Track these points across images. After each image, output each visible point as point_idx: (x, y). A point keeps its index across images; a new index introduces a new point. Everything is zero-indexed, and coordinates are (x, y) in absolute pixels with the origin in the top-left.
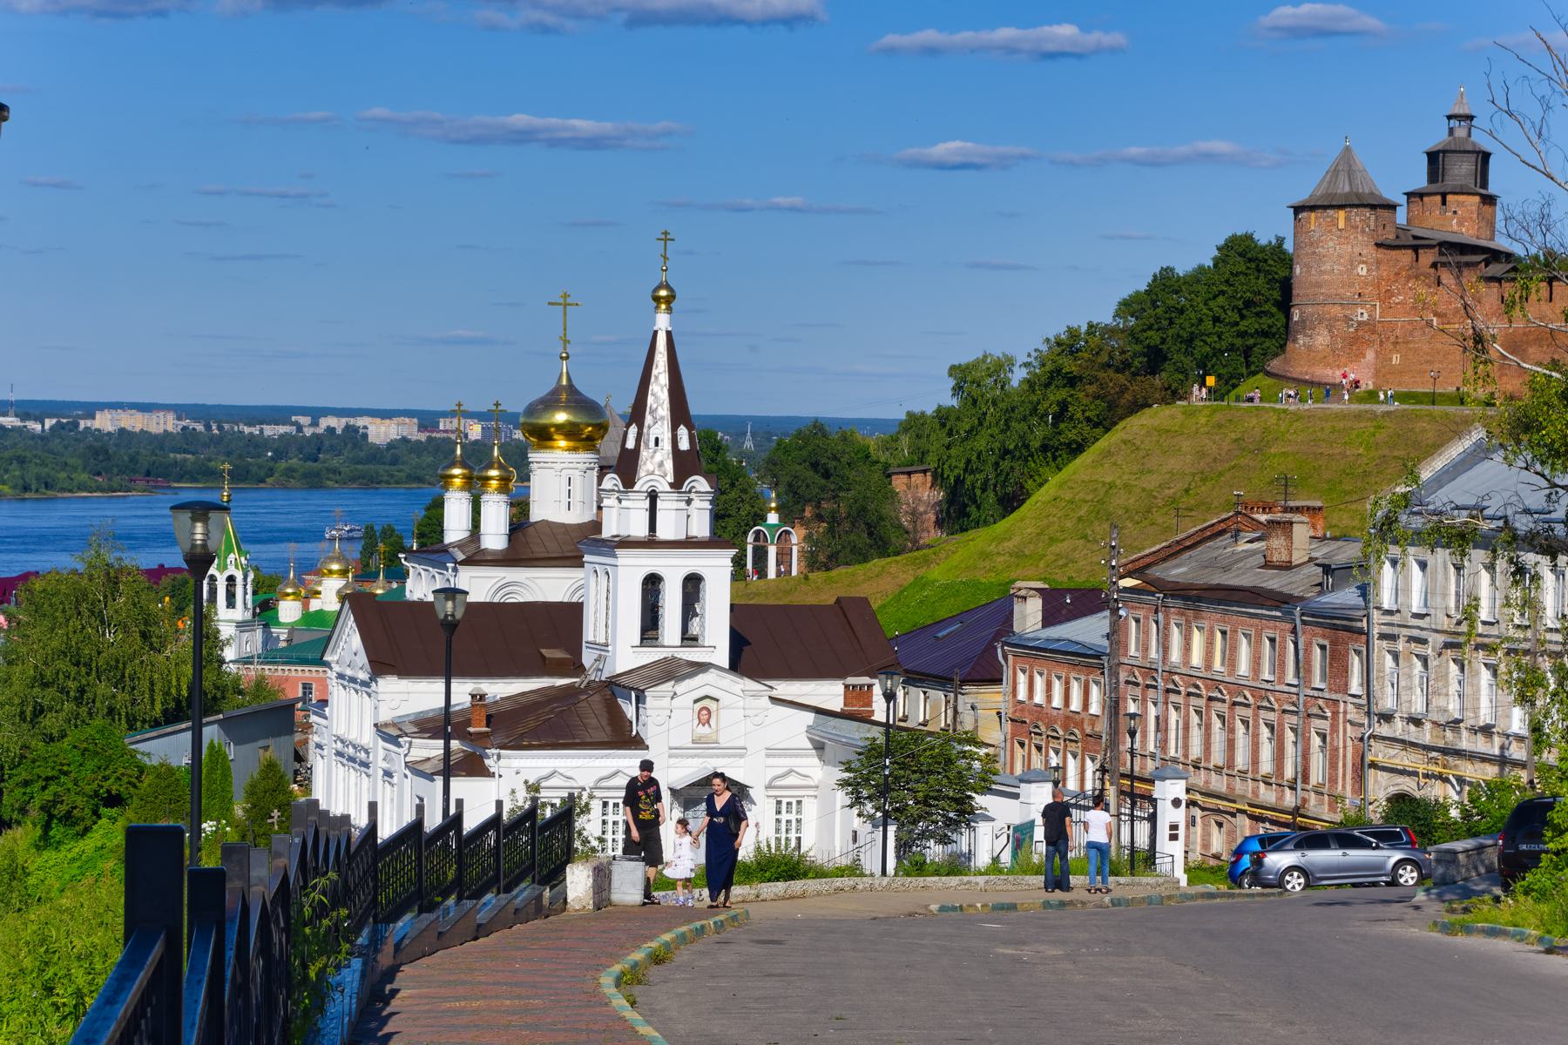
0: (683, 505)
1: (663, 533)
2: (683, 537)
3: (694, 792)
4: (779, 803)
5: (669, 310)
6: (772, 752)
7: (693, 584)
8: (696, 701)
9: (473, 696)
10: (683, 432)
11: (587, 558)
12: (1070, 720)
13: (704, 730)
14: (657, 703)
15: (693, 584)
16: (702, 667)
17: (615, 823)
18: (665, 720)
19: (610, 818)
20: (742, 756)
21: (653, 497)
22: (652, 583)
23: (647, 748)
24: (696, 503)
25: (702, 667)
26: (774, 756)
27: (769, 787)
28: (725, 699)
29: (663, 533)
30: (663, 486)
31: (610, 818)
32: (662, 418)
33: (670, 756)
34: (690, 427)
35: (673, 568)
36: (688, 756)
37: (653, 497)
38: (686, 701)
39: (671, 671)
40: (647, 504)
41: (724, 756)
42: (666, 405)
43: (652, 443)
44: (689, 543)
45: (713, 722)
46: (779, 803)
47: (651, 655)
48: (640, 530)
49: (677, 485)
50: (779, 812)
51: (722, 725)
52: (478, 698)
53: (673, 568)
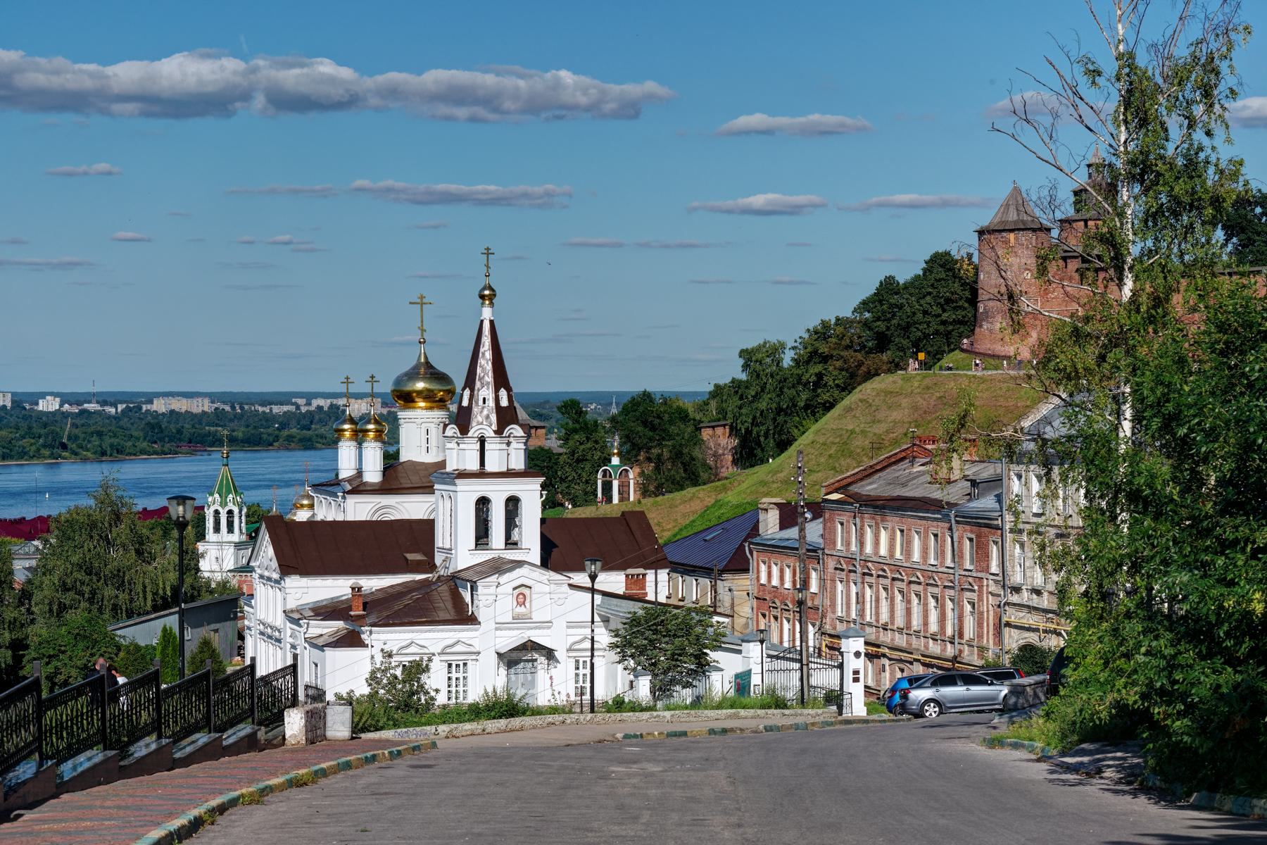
0: (504, 446)
1: (489, 468)
2: (505, 469)
3: (515, 655)
4: (577, 662)
5: (492, 304)
7: (513, 504)
9: (353, 589)
10: (503, 393)
11: (436, 487)
13: (521, 610)
14: (487, 591)
15: (513, 504)
16: (519, 564)
18: (492, 600)
19: (454, 675)
21: (482, 441)
22: (483, 503)
24: (514, 445)
25: (519, 564)
28: (537, 588)
29: (489, 468)
30: (489, 432)
32: (488, 383)
33: (497, 629)
34: (509, 390)
35: (498, 493)
36: (510, 629)
37: (482, 441)
39: (498, 567)
40: (478, 446)
41: (536, 628)
42: (491, 374)
43: (481, 402)
44: (510, 474)
45: (527, 604)
46: (577, 662)
47: (483, 556)
48: (474, 466)
49: (499, 432)
50: (577, 668)
52: (356, 590)
53: (498, 493)
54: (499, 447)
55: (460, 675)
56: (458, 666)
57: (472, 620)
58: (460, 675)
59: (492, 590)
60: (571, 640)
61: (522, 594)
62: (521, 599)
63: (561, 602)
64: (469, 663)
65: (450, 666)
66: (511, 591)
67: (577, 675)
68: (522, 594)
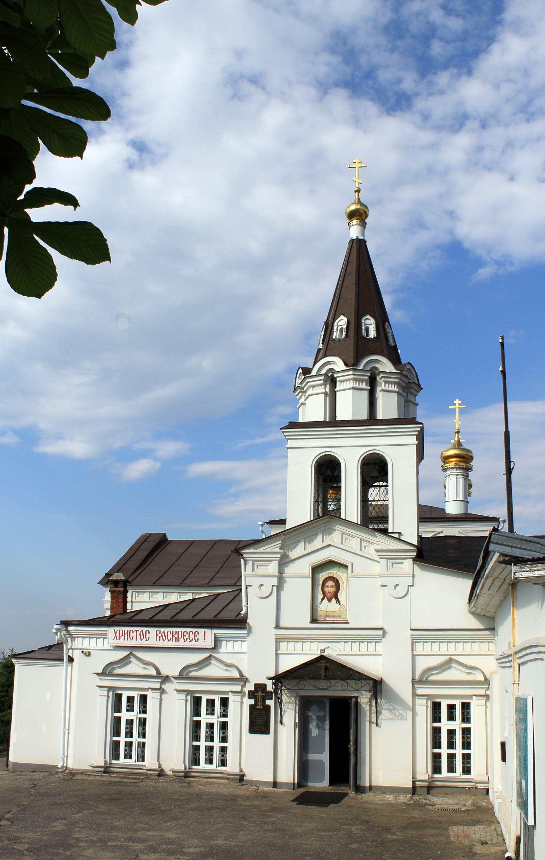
4: (436, 706)
6: (420, 636)
8: (316, 569)
14: (261, 570)
20: (378, 640)
26: (425, 640)
27: (417, 682)
28: (359, 565)
46: (436, 706)
50: (436, 718)
54: (351, 384)
55: (215, 719)
56: (211, 703)
58: (215, 719)
60: (422, 664)
61: (326, 580)
62: (330, 587)
63: (401, 590)
64: (232, 698)
65: (197, 702)
66: (308, 571)
67: (437, 732)
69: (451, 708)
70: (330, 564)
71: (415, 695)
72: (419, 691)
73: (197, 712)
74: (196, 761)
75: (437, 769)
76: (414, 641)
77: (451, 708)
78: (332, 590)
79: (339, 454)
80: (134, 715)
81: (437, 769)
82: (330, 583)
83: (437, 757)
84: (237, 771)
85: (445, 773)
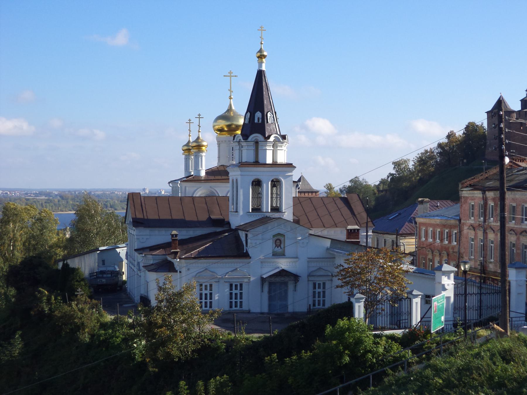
3: (273, 279)
4: (315, 284)
8: (274, 236)
12: (446, 249)
13: (278, 250)
15: (276, 183)
17: (236, 294)
21: (257, 143)
23: (250, 258)
27: (309, 275)
31: (204, 292)
38: (270, 234)
45: (282, 246)
47: (257, 216)
50: (315, 288)
51: (286, 246)
57: (246, 255)
58: (238, 292)
59: (260, 236)
61: (279, 240)
62: (278, 243)
65: (231, 285)
67: (314, 292)
68: (279, 240)
69: (319, 284)
70: (279, 234)
71: (308, 280)
72: (310, 279)
73: (231, 289)
74: (231, 307)
75: (314, 305)
76: (308, 262)
77: (319, 284)
78: (279, 243)
79: (260, 178)
80: (204, 292)
81: (314, 305)
82: (278, 241)
83: (314, 301)
84: (247, 309)
85: (317, 306)
